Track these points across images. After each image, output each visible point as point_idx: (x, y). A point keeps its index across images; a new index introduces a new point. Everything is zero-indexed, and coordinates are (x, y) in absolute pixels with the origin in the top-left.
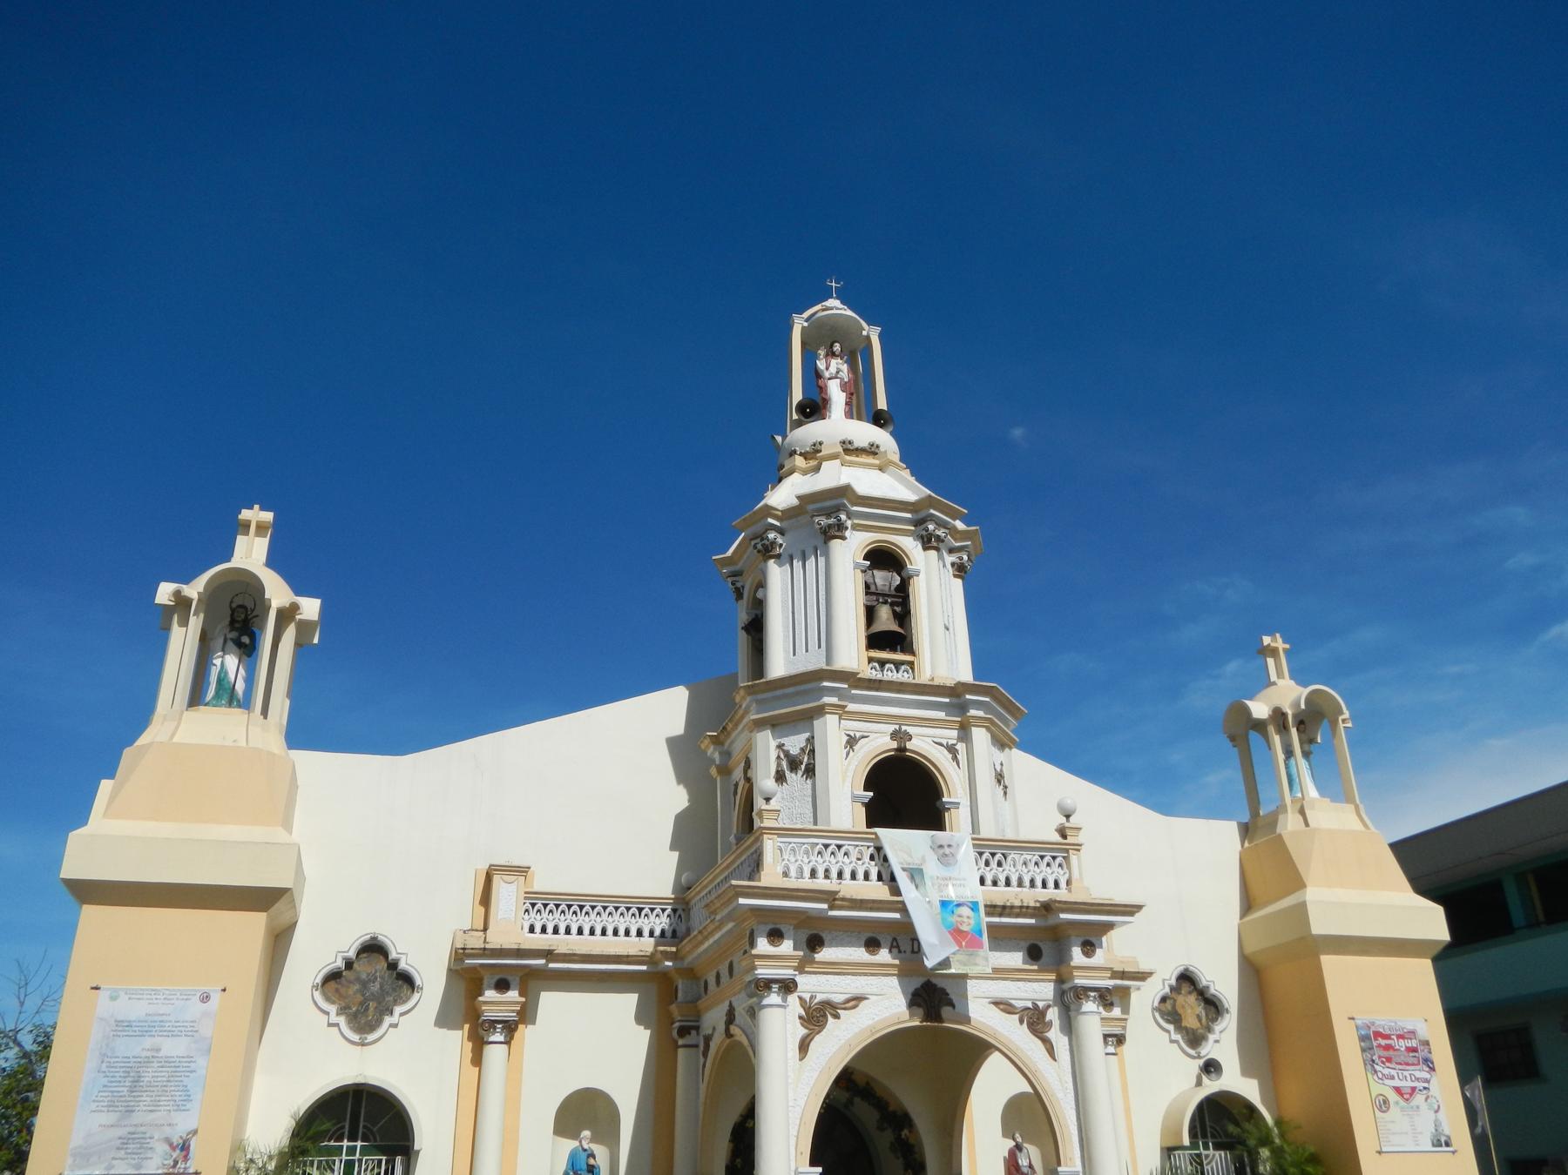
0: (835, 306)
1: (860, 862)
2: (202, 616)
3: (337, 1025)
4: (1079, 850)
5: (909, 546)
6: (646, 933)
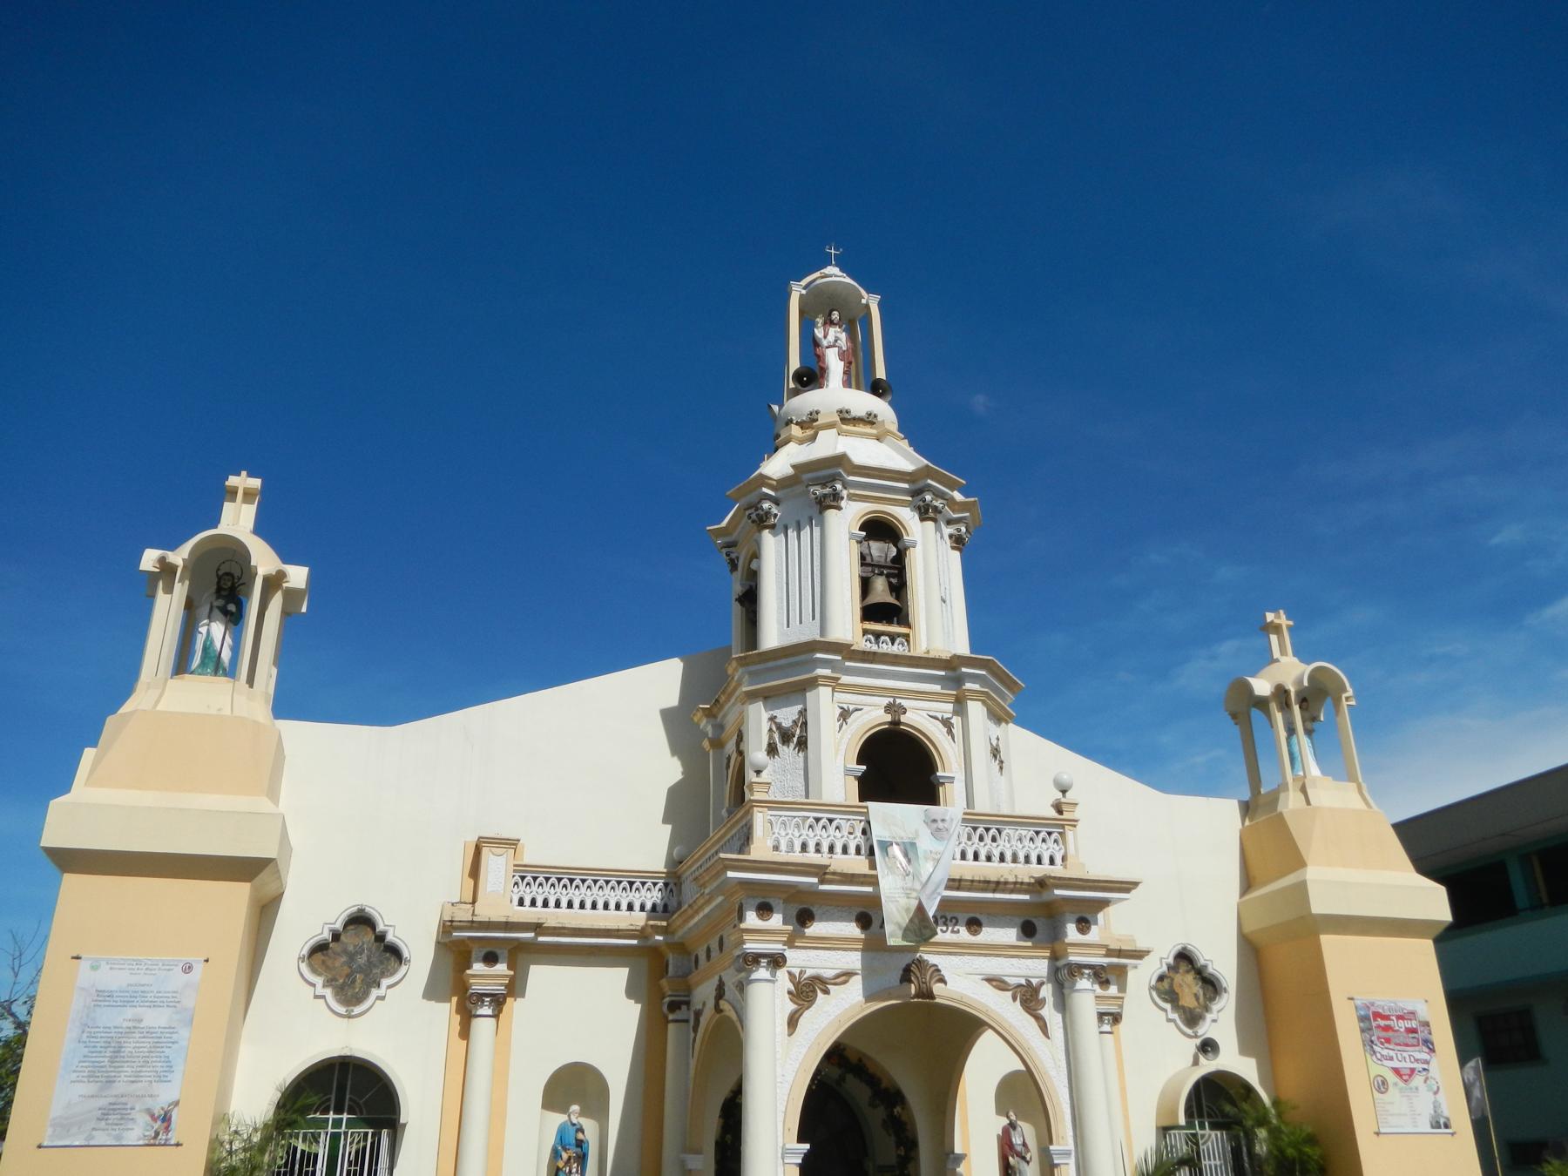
0: (834, 274)
1: (852, 836)
2: (187, 583)
3: (323, 997)
4: (1075, 826)
5: (906, 516)
6: (637, 907)
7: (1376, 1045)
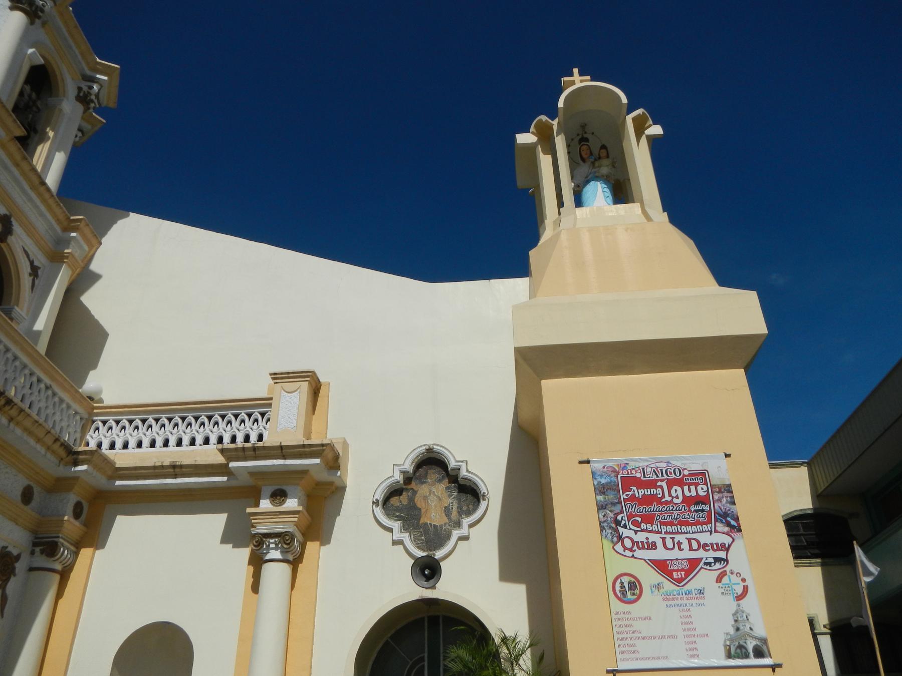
7: (625, 527)
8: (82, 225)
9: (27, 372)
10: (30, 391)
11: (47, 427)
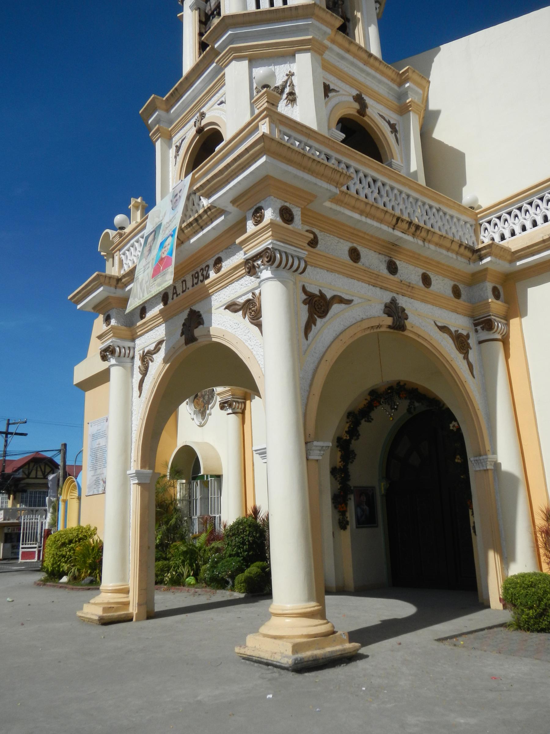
8: (410, 74)
9: (419, 203)
10: (428, 217)
11: (450, 238)
